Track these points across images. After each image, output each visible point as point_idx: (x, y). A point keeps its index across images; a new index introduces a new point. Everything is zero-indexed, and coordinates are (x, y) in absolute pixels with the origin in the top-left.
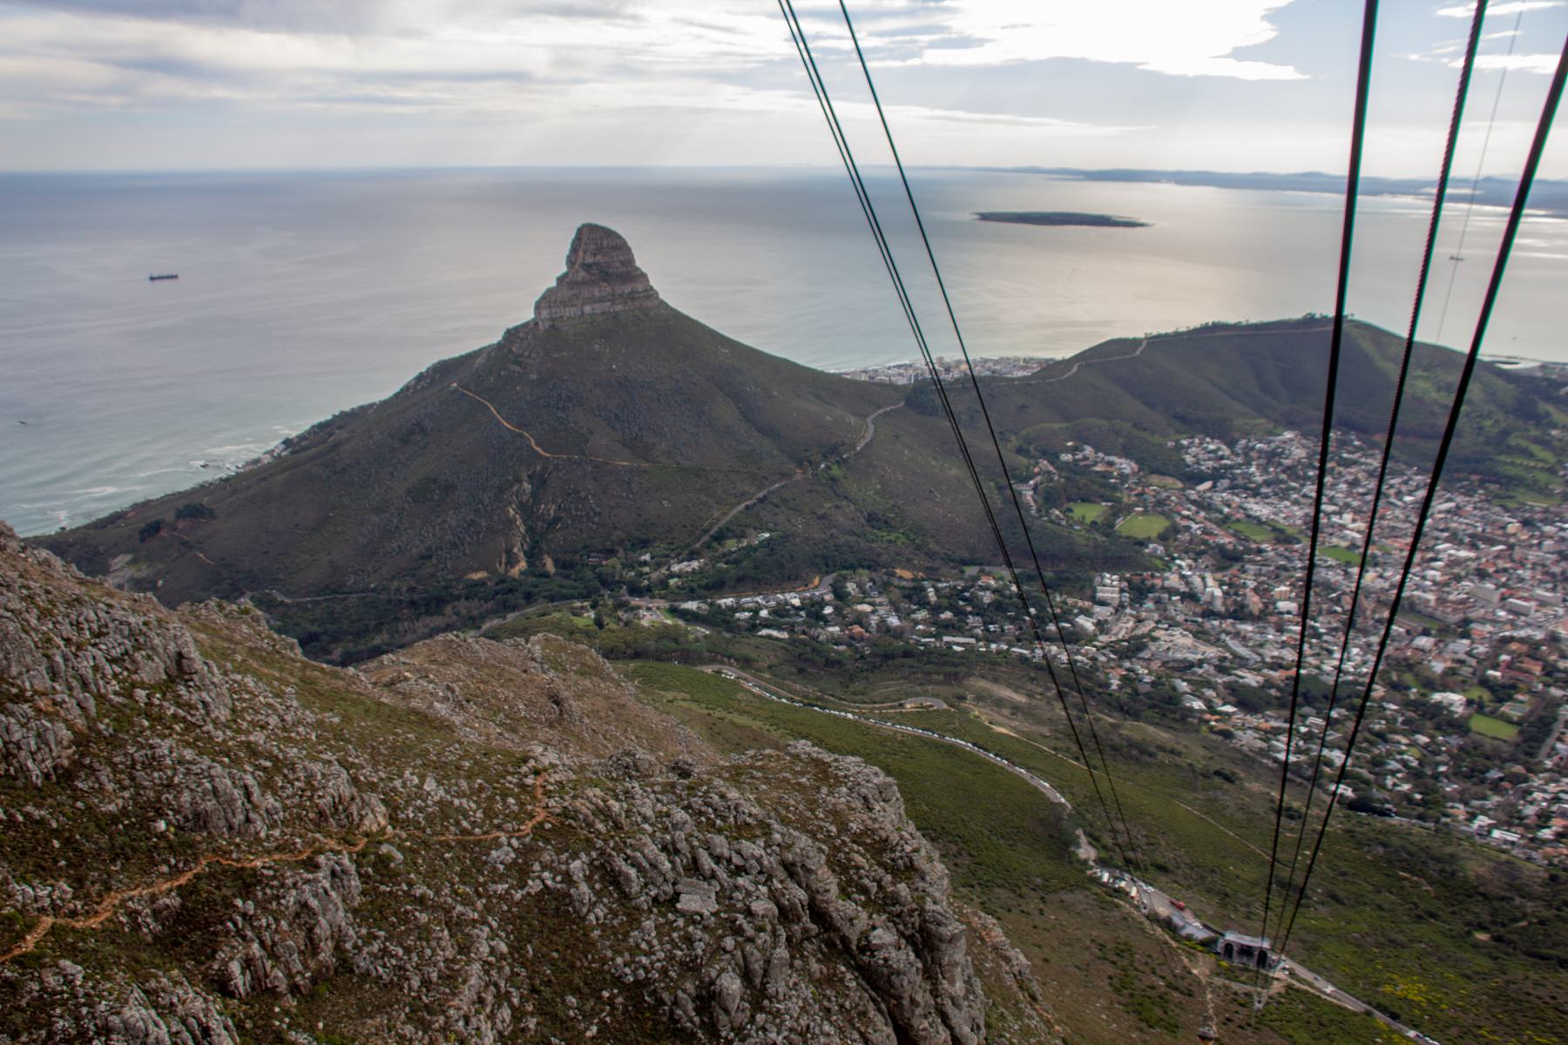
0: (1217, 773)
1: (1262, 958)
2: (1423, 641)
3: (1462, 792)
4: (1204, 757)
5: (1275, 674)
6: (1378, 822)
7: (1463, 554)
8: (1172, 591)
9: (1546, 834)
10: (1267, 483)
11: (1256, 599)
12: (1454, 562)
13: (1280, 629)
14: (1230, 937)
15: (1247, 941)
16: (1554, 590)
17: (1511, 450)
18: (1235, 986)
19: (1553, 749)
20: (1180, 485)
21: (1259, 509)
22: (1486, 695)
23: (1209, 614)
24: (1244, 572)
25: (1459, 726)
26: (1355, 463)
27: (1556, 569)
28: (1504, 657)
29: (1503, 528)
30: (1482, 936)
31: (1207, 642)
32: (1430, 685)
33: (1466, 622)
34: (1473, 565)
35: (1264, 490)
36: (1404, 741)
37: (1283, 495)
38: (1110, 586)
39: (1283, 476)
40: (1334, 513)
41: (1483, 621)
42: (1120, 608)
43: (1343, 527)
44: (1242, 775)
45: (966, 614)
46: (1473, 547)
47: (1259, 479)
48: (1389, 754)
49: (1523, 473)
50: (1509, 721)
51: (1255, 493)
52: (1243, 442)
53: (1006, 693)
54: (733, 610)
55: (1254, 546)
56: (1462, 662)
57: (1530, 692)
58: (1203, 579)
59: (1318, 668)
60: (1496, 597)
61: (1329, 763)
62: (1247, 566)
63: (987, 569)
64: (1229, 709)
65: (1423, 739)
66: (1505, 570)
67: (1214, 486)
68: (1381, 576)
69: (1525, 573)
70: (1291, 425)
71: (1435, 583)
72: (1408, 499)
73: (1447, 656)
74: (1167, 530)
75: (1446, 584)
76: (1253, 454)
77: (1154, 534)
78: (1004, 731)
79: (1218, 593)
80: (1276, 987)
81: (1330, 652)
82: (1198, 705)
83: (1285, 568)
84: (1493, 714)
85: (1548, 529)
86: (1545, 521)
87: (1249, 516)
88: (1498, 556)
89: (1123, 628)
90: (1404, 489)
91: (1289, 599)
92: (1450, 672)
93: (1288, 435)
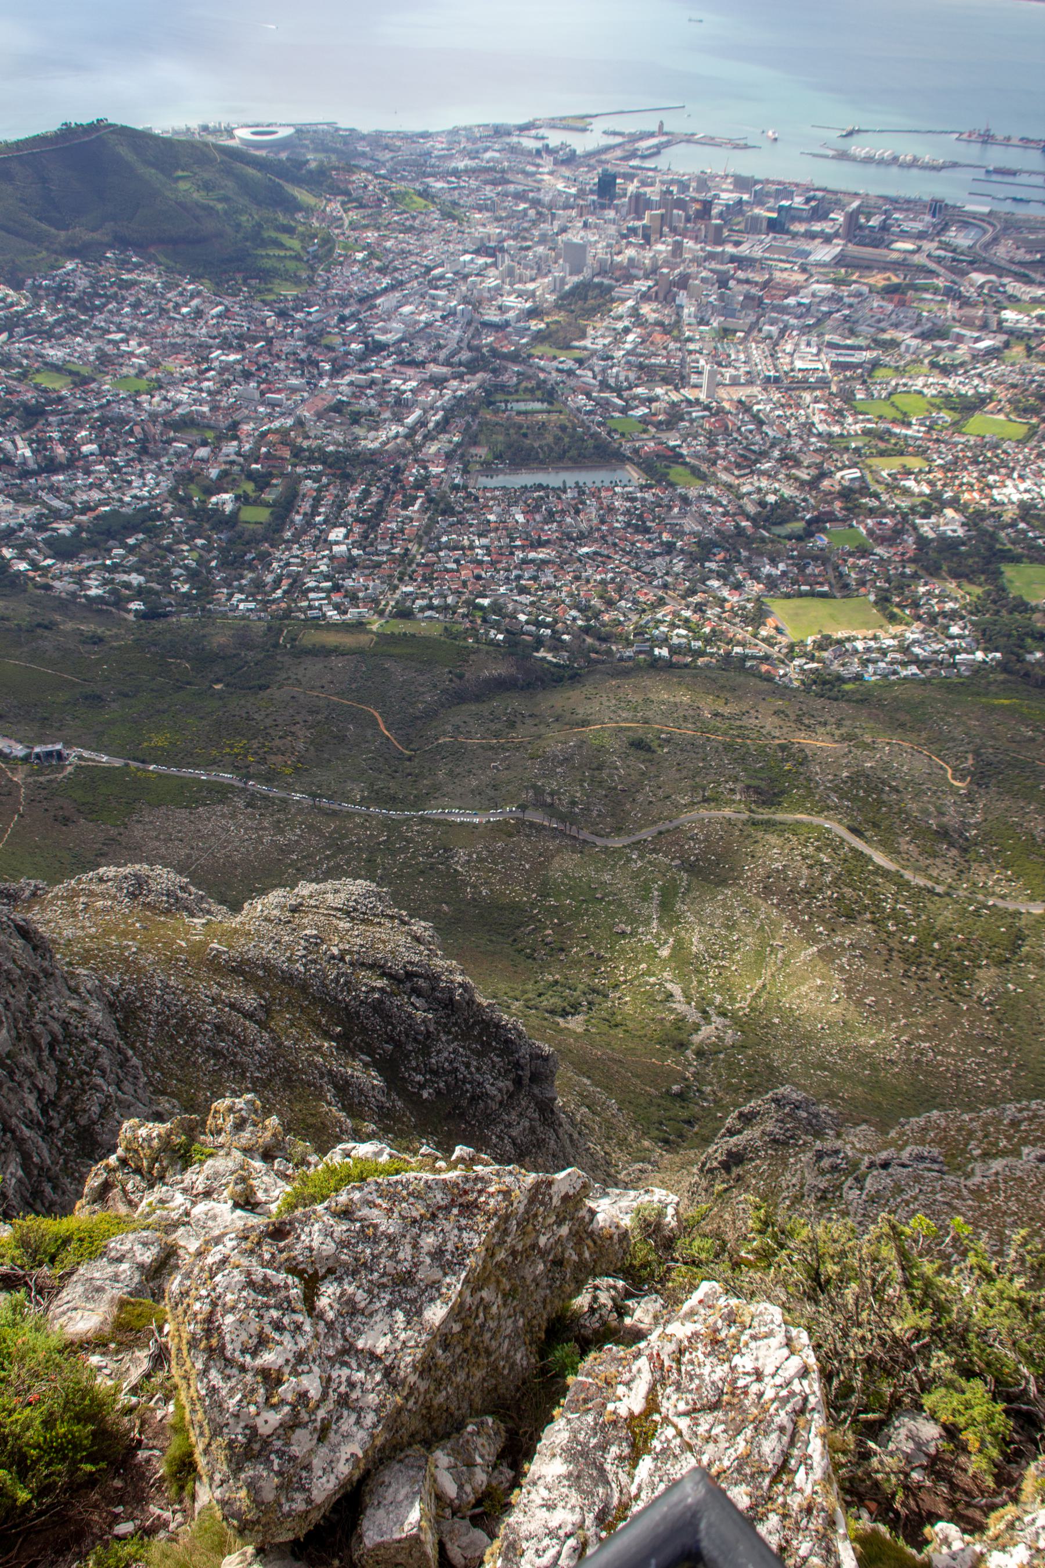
0: (39, 625)
1: (59, 755)
2: (202, 452)
3: (223, 579)
4: (30, 615)
5: (84, 518)
6: (159, 625)
7: (232, 358)
9: (279, 593)
10: (58, 323)
11: (60, 450)
12: (226, 368)
13: (88, 473)
14: (37, 750)
15: (50, 748)
16: (302, 375)
17: (264, 243)
18: (41, 779)
19: (292, 522)
21: (55, 353)
22: (249, 487)
23: (25, 474)
24: (49, 425)
25: (231, 521)
26: (134, 283)
27: (303, 356)
28: (264, 450)
29: (264, 323)
30: (218, 687)
31: (29, 502)
32: (210, 490)
33: (235, 426)
34: (239, 367)
35: (57, 330)
36: (186, 547)
37: (75, 330)
39: (73, 311)
40: (122, 341)
41: (247, 419)
43: (132, 354)
44: (58, 618)
46: (241, 348)
47: (50, 319)
48: (175, 564)
49: (279, 265)
50: (267, 505)
51: (48, 335)
52: (30, 281)
55: (54, 396)
56: (232, 463)
57: (282, 475)
58: (14, 442)
59: (121, 500)
60: (257, 395)
61: (127, 585)
62: (51, 419)
64: (50, 562)
65: (200, 542)
66: (265, 366)
67: (11, 336)
68: (165, 399)
69: (280, 365)
70: (72, 253)
71: (210, 393)
72: (185, 310)
73: (221, 459)
75: (218, 392)
76: (42, 293)
79: (28, 453)
80: (70, 769)
81: (130, 483)
82: (23, 566)
83: (83, 411)
84: (257, 502)
85: (299, 316)
86: (296, 309)
87: (46, 364)
88: (259, 353)
90: (180, 300)
91: (91, 442)
92: (224, 474)
93: (70, 266)
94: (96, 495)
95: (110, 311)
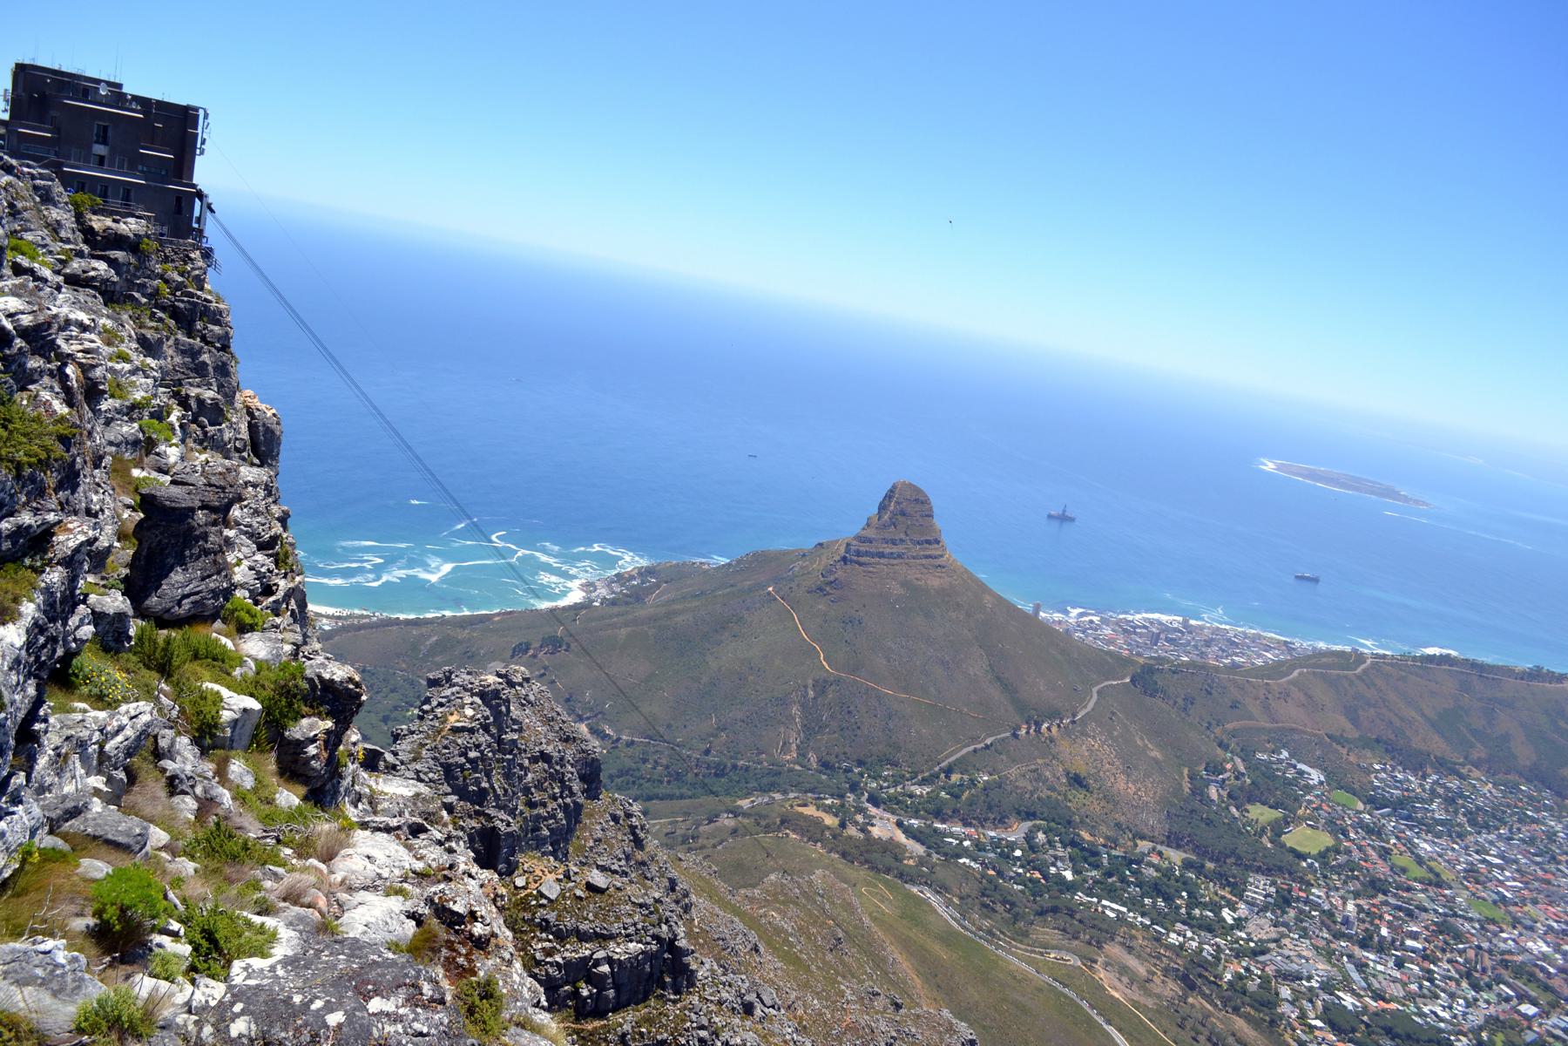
8: (1316, 906)
11: (1384, 932)
13: (1399, 964)
20: (1360, 806)
21: (1425, 847)
23: (1338, 936)
38: (1259, 887)
40: (1497, 866)
42: (1264, 909)
45: (1128, 884)
53: (1132, 962)
54: (944, 834)
63: (1159, 847)
64: (1318, 1023)
74: (1328, 849)
77: (1314, 852)
78: (1116, 995)
83: (1426, 910)
89: (1261, 929)
94: (1396, 990)
95: (1500, 836)
